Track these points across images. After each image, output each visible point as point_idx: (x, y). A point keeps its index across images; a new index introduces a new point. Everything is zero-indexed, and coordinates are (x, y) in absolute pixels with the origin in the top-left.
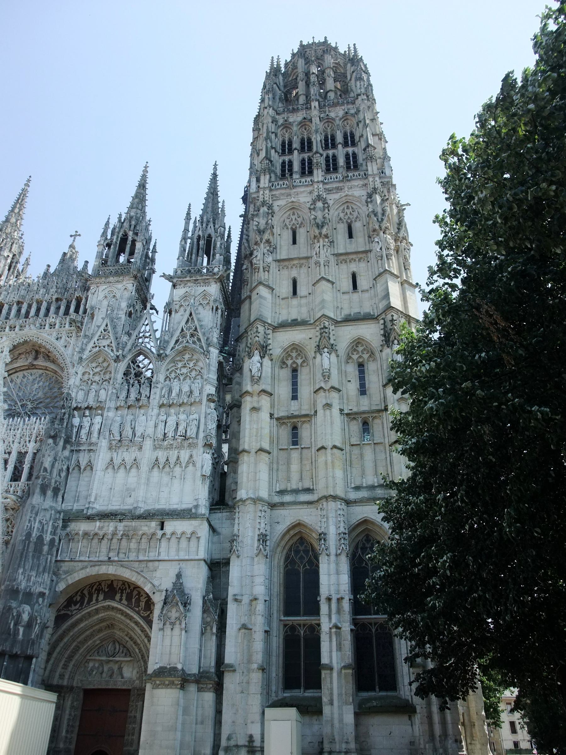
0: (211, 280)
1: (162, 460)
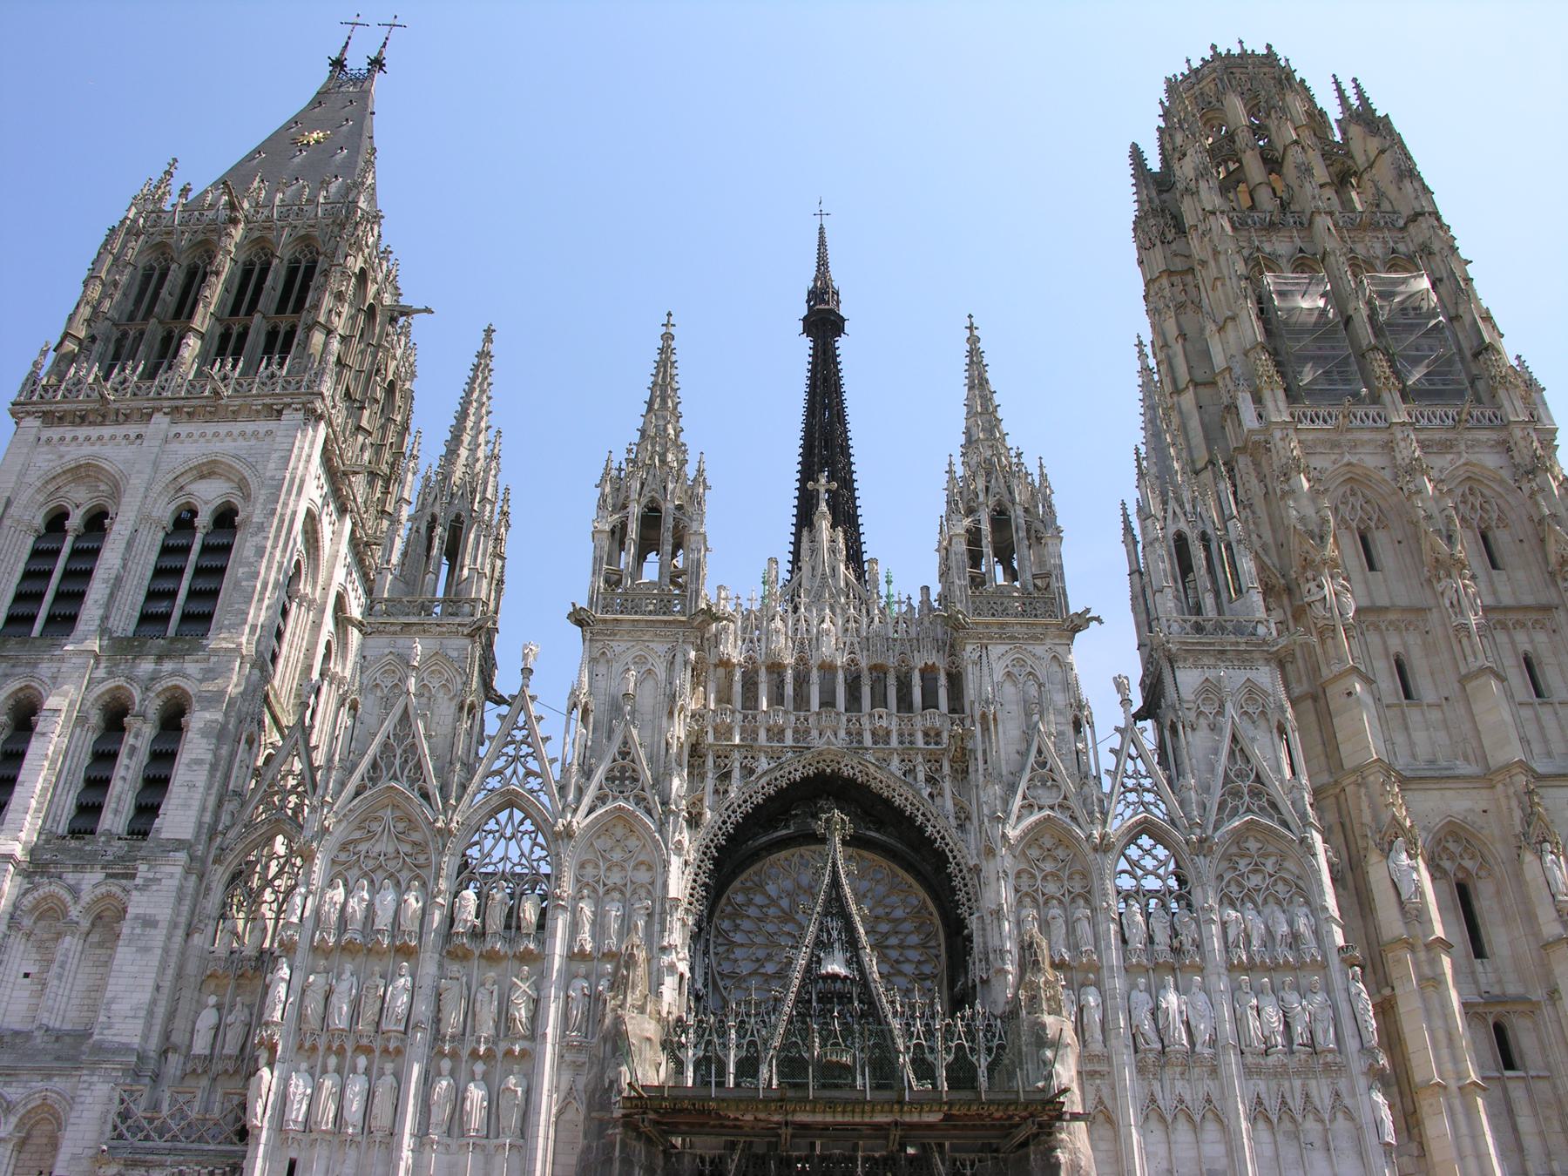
0: (1256, 655)
1: (1272, 1104)
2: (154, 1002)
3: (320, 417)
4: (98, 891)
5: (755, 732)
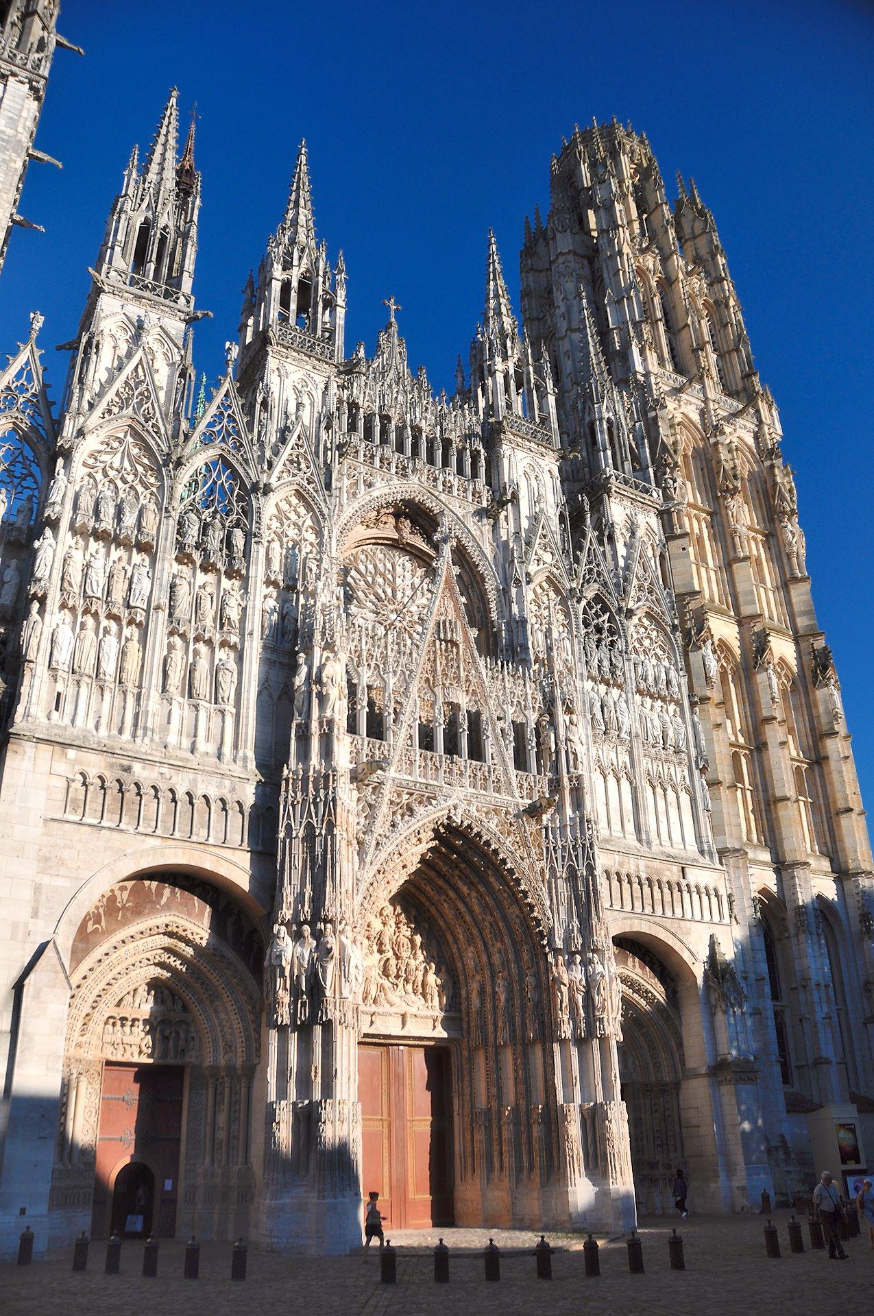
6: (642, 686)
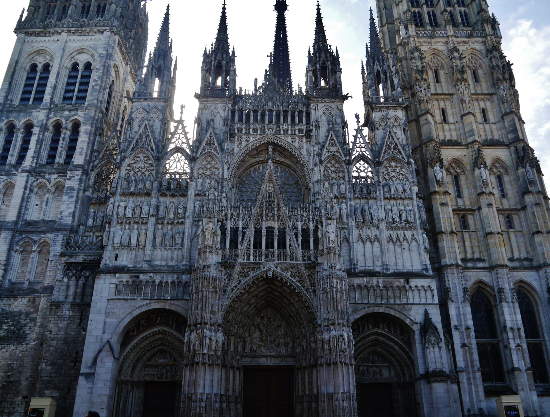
2: (75, 212)
3: (116, 34)
4: (56, 180)
5: (249, 130)
6: (387, 195)
